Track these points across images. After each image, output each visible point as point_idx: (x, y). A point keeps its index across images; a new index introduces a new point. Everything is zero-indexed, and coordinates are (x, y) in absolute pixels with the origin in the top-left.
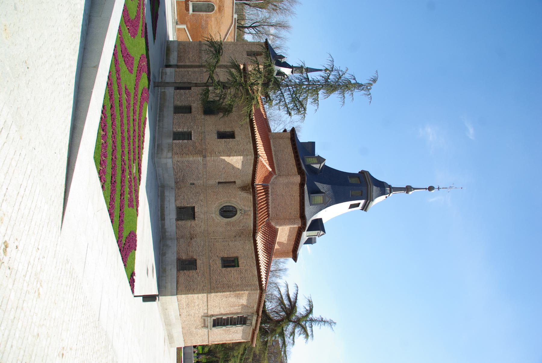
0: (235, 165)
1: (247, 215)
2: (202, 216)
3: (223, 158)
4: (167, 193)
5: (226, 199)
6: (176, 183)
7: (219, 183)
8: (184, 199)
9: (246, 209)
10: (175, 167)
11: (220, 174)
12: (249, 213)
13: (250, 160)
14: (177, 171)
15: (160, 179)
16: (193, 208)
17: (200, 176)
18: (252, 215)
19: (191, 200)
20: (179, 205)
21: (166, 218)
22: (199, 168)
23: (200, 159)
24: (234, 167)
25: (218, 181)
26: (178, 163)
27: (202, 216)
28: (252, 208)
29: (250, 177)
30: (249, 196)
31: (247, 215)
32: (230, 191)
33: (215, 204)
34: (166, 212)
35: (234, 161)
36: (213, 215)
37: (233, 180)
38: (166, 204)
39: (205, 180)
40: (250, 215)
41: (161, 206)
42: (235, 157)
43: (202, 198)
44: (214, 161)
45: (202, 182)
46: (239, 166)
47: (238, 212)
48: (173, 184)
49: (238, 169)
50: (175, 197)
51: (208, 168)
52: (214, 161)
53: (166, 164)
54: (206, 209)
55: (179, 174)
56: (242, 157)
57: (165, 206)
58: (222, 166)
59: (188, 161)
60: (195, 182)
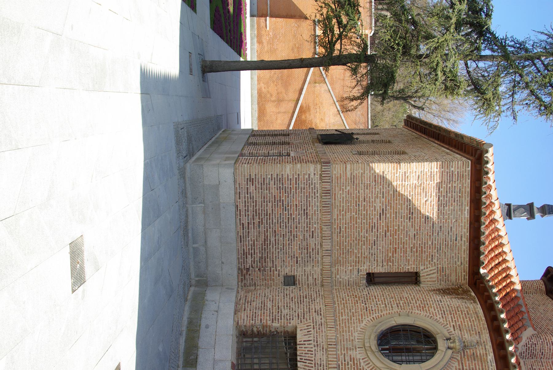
0: (416, 203)
1: (474, 357)
2: (320, 356)
3: (380, 168)
4: (212, 296)
5: (396, 309)
6: (243, 273)
7: (372, 279)
8: (264, 305)
9: (467, 336)
10: (241, 207)
11: (372, 238)
12: (480, 351)
13: (461, 176)
14: (245, 221)
15: (196, 250)
16: (291, 338)
17: (312, 242)
18: (491, 356)
19: (285, 311)
20: (246, 320)
21: (201, 359)
22: (310, 211)
23: (312, 170)
24: (412, 211)
25: (365, 268)
26: (252, 188)
27: (320, 356)
28: (486, 336)
29: (464, 255)
30: (471, 306)
31: (474, 357)
32: (405, 295)
33: (360, 321)
34: (204, 340)
35: (413, 181)
36: (358, 354)
37: (410, 268)
38: (207, 318)
39: (327, 260)
40: (482, 359)
41: (191, 322)
42: (414, 165)
43: (319, 304)
44: (353, 179)
45: (318, 269)
46: (428, 205)
47: (442, 345)
48: (229, 271)
49: (427, 218)
50: (237, 304)
51: (336, 212)
52: (353, 179)
53: (217, 187)
54: (331, 334)
55: (253, 233)
56: (434, 164)
57: (203, 323)
58: (378, 205)
59: (279, 180)
60: (298, 272)
